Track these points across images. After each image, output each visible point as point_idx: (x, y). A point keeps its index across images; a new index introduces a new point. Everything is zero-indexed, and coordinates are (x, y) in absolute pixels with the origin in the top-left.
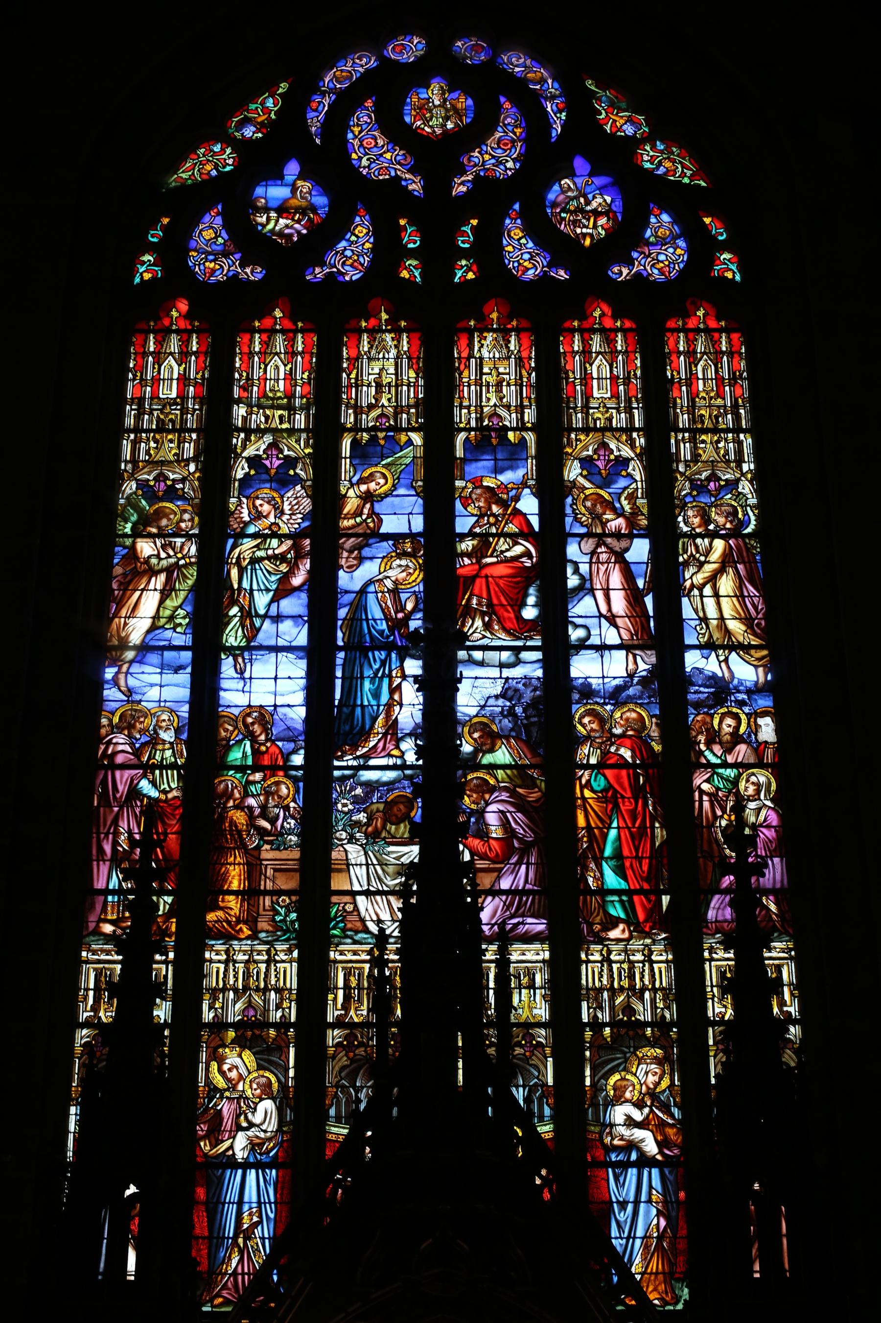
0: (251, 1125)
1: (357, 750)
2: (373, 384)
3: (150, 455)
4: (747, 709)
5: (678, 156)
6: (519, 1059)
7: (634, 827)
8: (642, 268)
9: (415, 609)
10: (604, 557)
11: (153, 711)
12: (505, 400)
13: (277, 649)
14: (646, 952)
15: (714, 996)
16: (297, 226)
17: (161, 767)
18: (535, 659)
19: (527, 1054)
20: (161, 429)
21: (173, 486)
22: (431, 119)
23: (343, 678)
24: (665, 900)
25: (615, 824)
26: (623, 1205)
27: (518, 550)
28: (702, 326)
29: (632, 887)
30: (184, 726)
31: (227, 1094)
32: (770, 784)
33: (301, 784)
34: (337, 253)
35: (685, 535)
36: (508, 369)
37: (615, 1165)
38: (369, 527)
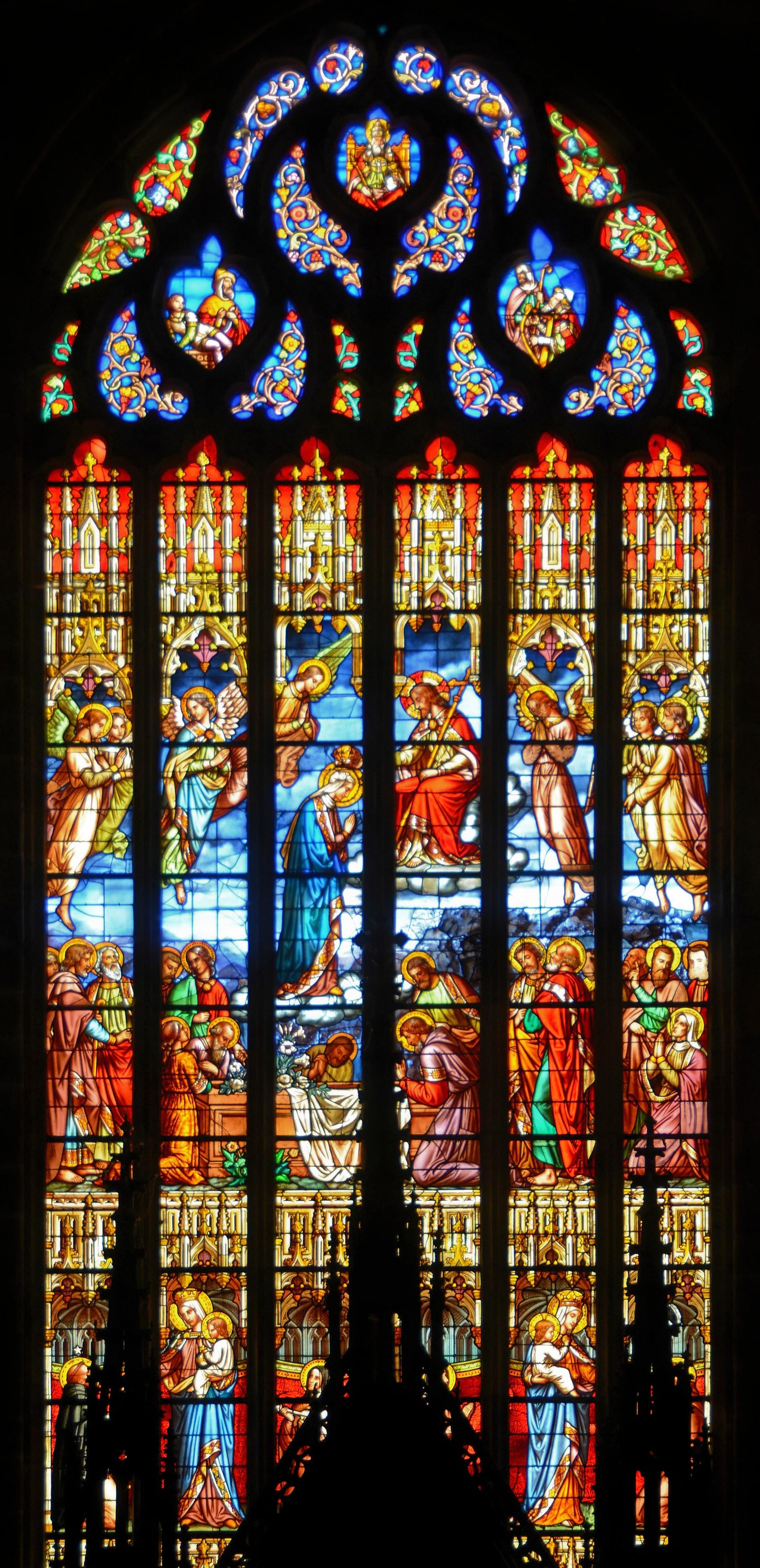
0: (210, 1364)
1: (297, 988)
2: (309, 554)
3: (76, 647)
4: (681, 943)
5: (653, 228)
8: (603, 394)
9: (354, 831)
10: (546, 768)
11: (98, 947)
12: (448, 574)
13: (216, 876)
14: (570, 1197)
16: (221, 336)
17: (110, 1008)
18: (473, 887)
20: (85, 613)
21: (101, 684)
22: (369, 175)
23: (284, 909)
25: (546, 1067)
27: (459, 760)
28: (664, 474)
29: (560, 1133)
30: (129, 963)
31: (187, 1335)
33: (245, 1025)
34: (265, 375)
35: (631, 742)
37: (534, 1400)
38: (306, 734)
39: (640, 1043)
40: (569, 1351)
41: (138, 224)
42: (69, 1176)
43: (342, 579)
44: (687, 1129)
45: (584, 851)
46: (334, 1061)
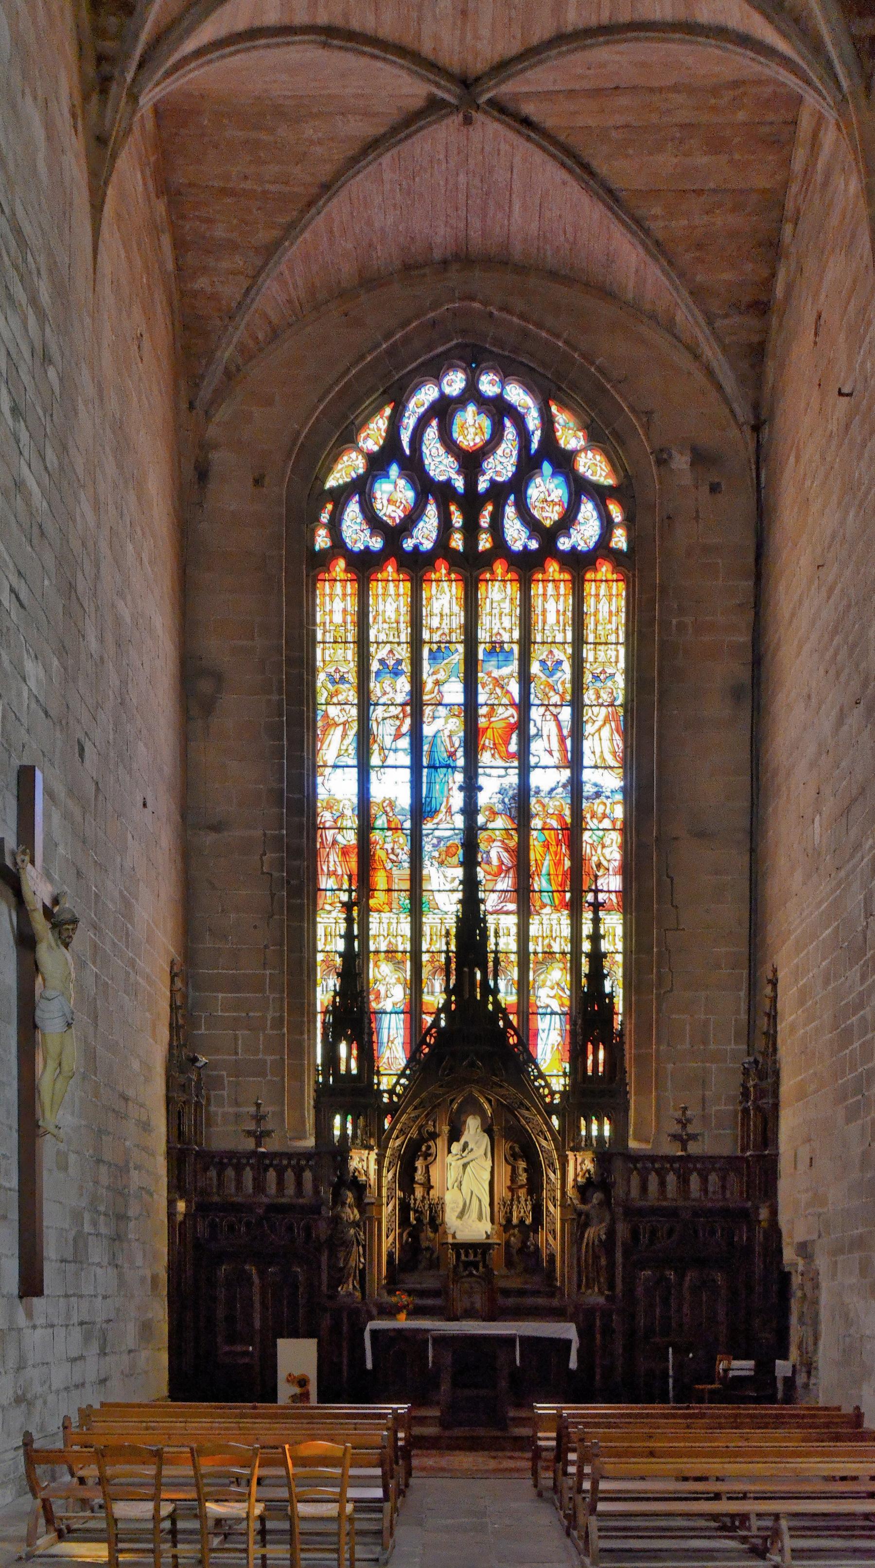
4: (610, 800)
10: (549, 717)
13: (396, 767)
20: (335, 642)
26: (543, 1031)
36: (506, 605)
41: (360, 457)
42: (328, 907)
43: (454, 626)
44: (612, 888)
45: (566, 756)
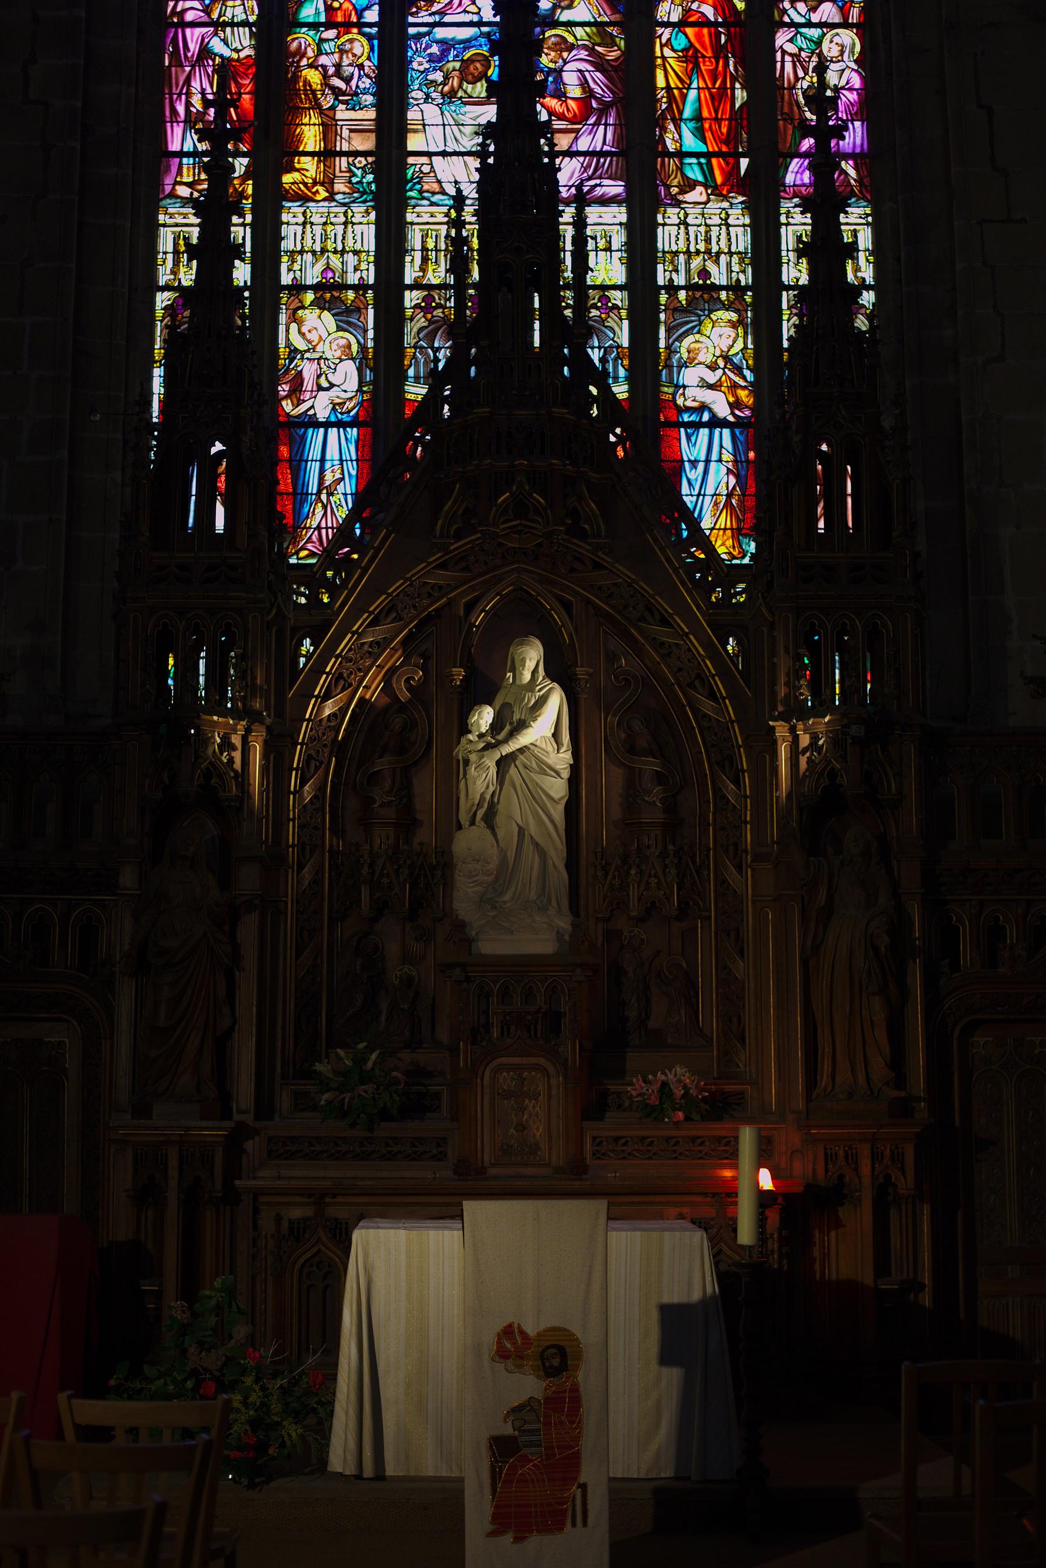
0: (332, 386)
1: (432, 6)
6: (595, 321)
7: (714, 88)
14: (723, 216)
15: (789, 260)
17: (233, 24)
19: (603, 316)
24: (744, 163)
25: (695, 85)
26: (694, 463)
29: (711, 150)
31: (307, 355)
32: (854, 44)
33: (376, 42)
37: (687, 425)
39: (793, 62)
40: (724, 373)
46: (470, 78)
